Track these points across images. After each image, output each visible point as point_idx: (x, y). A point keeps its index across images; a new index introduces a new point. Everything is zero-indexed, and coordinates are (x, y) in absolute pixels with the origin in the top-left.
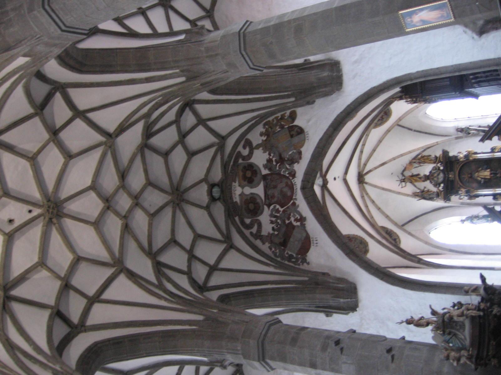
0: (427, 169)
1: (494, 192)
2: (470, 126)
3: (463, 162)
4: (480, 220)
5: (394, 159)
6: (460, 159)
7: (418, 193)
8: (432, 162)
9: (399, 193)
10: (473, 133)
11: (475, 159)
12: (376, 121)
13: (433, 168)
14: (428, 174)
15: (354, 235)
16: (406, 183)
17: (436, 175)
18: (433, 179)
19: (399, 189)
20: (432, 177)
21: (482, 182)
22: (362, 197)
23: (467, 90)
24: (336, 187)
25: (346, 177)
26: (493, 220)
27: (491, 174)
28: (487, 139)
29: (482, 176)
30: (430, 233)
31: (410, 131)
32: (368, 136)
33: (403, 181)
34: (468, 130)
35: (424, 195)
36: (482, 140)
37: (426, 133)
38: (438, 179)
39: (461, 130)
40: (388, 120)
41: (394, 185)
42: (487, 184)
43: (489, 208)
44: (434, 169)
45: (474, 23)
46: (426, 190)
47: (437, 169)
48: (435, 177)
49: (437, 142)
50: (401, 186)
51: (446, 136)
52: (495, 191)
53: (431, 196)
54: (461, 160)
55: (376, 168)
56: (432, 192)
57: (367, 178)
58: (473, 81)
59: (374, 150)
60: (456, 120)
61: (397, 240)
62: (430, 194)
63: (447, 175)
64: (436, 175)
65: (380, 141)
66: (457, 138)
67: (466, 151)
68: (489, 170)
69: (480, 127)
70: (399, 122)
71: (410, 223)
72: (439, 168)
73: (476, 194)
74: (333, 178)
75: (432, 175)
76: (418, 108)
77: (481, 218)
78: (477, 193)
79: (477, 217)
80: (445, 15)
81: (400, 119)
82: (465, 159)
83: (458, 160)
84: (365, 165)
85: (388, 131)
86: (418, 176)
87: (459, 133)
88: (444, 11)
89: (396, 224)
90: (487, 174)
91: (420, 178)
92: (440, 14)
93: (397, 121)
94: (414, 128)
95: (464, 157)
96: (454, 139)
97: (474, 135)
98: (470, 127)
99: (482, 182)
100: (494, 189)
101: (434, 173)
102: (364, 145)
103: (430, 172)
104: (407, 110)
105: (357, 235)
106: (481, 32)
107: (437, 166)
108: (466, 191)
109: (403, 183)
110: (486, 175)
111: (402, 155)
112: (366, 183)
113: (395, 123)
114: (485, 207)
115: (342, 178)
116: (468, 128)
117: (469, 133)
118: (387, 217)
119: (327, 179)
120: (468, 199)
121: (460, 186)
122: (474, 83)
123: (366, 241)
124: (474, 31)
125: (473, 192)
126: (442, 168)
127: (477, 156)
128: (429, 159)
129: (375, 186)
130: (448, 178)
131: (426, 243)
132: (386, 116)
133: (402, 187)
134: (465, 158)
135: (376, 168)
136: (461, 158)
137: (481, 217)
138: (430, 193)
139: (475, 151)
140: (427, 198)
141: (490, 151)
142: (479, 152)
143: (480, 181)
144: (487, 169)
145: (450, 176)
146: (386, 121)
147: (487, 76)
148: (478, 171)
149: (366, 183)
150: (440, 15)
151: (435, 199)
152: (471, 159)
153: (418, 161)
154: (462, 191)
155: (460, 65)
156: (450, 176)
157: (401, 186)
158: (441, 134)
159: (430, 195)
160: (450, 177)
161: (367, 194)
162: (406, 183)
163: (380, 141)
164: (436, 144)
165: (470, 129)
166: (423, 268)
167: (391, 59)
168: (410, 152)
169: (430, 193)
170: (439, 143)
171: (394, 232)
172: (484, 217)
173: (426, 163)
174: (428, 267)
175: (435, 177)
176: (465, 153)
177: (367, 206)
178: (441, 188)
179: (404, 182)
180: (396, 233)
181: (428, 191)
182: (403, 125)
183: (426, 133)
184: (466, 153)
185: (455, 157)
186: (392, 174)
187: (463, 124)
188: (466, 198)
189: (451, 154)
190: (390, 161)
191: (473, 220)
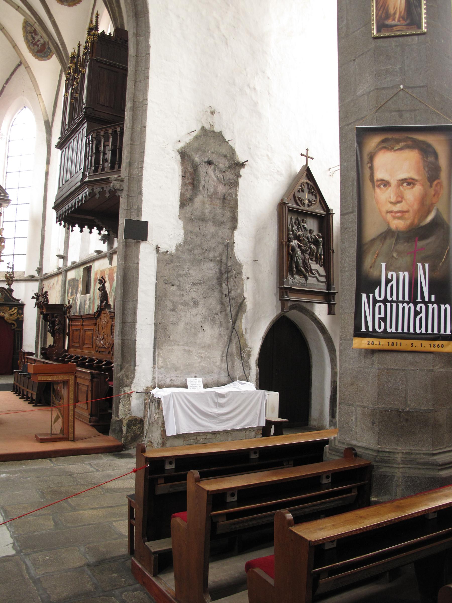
12: (37, 26)
23: (86, 125)
31: (5, 81)
32: (17, 10)
40: (30, 52)
45: (198, 150)
58: (102, 133)
60: (8, 141)
70: (24, 66)
80: (390, 22)
81: (27, 67)
85: (15, 46)
88: (399, 21)
92: (395, 14)
93: (26, 62)
104: (37, 80)
106: (184, 155)
113: (25, 59)
122: (98, 135)
124: (189, 145)
132: (36, 51)
146: (29, 47)
147: (104, 154)
150: (392, 11)
155: (146, 111)
167: (178, 17)
182: (18, 70)
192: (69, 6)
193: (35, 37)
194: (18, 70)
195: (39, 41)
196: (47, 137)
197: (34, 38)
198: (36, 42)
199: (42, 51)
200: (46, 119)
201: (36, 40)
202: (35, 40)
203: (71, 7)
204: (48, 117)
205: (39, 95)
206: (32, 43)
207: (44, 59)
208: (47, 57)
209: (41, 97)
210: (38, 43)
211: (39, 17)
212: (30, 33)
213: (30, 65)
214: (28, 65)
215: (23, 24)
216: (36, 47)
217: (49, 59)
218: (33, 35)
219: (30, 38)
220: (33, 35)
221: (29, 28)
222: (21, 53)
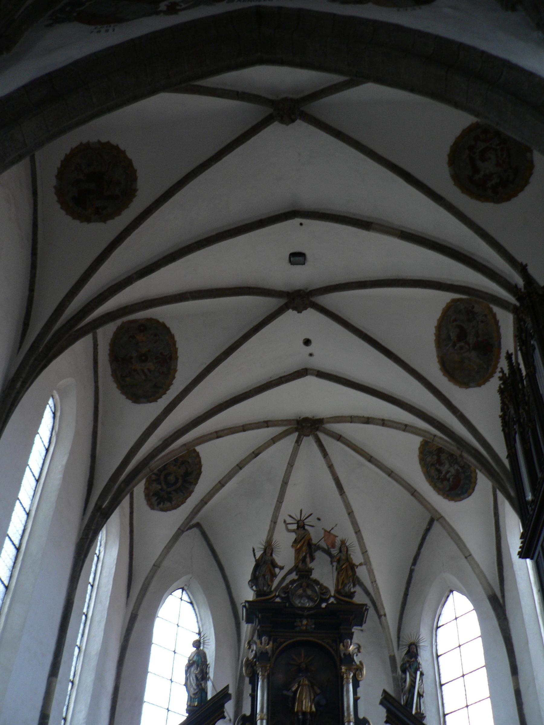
0: (324, 573)
1: (258, 717)
2: (422, 674)
3: (337, 650)
4: (193, 682)
5: (350, 513)
6: (344, 646)
7: (271, 555)
8: (340, 587)
9: (274, 522)
10: (405, 681)
11: (342, 678)
13: (326, 588)
14: (314, 576)
15: (175, 371)
16: (293, 531)
17: (309, 592)
18: (300, 586)
19: (283, 515)
20: (304, 584)
21: (285, 692)
22: (266, 424)
24: (286, 339)
25: (312, 374)
26: (190, 710)
27: (304, 713)
28: (389, 711)
29: (301, 693)
30: (183, 589)
33: (301, 525)
34: (413, 670)
35: (265, 566)
36: (387, 700)
37: (406, 595)
38: (301, 597)
39: (412, 652)
40: (439, 494)
41: (292, 507)
42: (280, 704)
43: (222, 706)
44: (324, 590)
46: (277, 570)
47: (324, 597)
48: (305, 591)
49: (385, 615)
50: (289, 520)
51: (399, 638)
52: (262, 719)
53: (261, 580)
54: (341, 646)
55: (331, 467)
56: (270, 583)
57: (309, 443)
59: (370, 459)
61: (168, 504)
62: (266, 577)
63: (306, 613)
64: (309, 592)
65: (390, 473)
66: (393, 659)
67: (361, 663)
68: (314, 709)
69: (420, 696)
71: (209, 553)
72: (326, 600)
73: (258, 674)
74: (311, 352)
75: (308, 586)
76: (466, 558)
77: (201, 684)
78: (260, 677)
79: (203, 676)
82: (342, 655)
83: (342, 641)
84: (339, 438)
85: (414, 492)
86: (308, 556)
87: (405, 650)
89: (204, 502)
90: (307, 705)
91: (304, 560)
94: (416, 568)
95: (347, 653)
96: (393, 654)
97: (399, 683)
98: (419, 673)
99: (285, 692)
100: (265, 717)
101: (314, 590)
102: (383, 423)
103: (316, 582)
105: (174, 377)
107: (331, 596)
108: (267, 653)
109: (294, 527)
110: (302, 702)
111: (358, 532)
112: (298, 442)
114: (223, 696)
115: (308, 366)
116: (417, 669)
117: (404, 671)
118: (221, 484)
119: (305, 308)
120: (248, 660)
121: (281, 643)
123: (160, 397)
125: (264, 668)
126: (324, 605)
127: (348, 683)
128: (346, 581)
129: (291, 464)
130: (301, 617)
131: (157, 566)
132: (447, 489)
133: (285, 521)
134: (344, 654)
135: (331, 467)
136: (347, 647)
137: (203, 685)
138: (268, 577)
139: (361, 683)
140: (257, 573)
141: (361, 716)
142: (359, 690)
143: (289, 689)
144: (318, 705)
145: (305, 622)
146: (435, 487)
148: (312, 685)
149: (298, 442)
151: (254, 588)
152: (343, 669)
153: (343, 558)
154: (268, 644)
156: (305, 622)
157: (289, 520)
158: (402, 628)
159: (264, 576)
160: (301, 622)
161: (274, 440)
162: (293, 531)
163: (390, 473)
164: (382, 613)
165: (416, 674)
166: (82, 519)
168: (364, 552)
169: (268, 577)
170: (383, 617)
171: (186, 498)
172: (202, 691)
173: (338, 573)
174: (84, 526)
175: (305, 591)
176: (357, 659)
177: (244, 428)
178: (278, 600)
179: (298, 527)
180: (183, 502)
181: (274, 575)
183: (406, 595)
184: (358, 663)
185: (350, 636)
186: (319, 519)
187: (424, 658)
188: (251, 656)
189: (355, 630)
190: (347, 505)
191: (198, 666)
192: (479, 385)
193: (441, 468)
194: (428, 538)
195: (448, 472)
196: (500, 625)
197: (439, 471)
198: (445, 476)
199: (457, 487)
200: (491, 593)
201: (444, 473)
202: (442, 473)
203: (483, 387)
204: (492, 589)
205: (468, 556)
206: (438, 479)
207: (462, 497)
208: (466, 492)
209: (473, 559)
210: (448, 476)
211: (438, 421)
212: (433, 465)
213: (443, 514)
214: (439, 514)
215: (419, 456)
216: (445, 483)
217: (470, 495)
218: (437, 466)
219: (433, 472)
220: (437, 466)
221: (429, 459)
222: (424, 499)
